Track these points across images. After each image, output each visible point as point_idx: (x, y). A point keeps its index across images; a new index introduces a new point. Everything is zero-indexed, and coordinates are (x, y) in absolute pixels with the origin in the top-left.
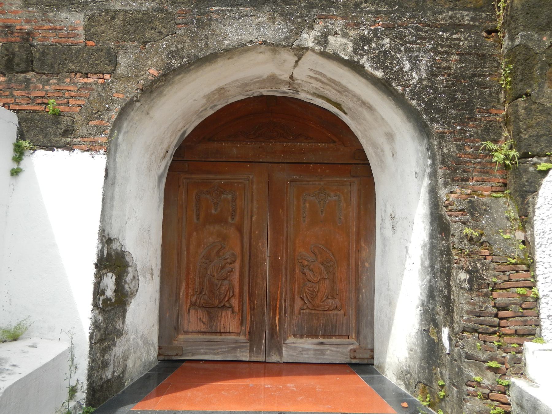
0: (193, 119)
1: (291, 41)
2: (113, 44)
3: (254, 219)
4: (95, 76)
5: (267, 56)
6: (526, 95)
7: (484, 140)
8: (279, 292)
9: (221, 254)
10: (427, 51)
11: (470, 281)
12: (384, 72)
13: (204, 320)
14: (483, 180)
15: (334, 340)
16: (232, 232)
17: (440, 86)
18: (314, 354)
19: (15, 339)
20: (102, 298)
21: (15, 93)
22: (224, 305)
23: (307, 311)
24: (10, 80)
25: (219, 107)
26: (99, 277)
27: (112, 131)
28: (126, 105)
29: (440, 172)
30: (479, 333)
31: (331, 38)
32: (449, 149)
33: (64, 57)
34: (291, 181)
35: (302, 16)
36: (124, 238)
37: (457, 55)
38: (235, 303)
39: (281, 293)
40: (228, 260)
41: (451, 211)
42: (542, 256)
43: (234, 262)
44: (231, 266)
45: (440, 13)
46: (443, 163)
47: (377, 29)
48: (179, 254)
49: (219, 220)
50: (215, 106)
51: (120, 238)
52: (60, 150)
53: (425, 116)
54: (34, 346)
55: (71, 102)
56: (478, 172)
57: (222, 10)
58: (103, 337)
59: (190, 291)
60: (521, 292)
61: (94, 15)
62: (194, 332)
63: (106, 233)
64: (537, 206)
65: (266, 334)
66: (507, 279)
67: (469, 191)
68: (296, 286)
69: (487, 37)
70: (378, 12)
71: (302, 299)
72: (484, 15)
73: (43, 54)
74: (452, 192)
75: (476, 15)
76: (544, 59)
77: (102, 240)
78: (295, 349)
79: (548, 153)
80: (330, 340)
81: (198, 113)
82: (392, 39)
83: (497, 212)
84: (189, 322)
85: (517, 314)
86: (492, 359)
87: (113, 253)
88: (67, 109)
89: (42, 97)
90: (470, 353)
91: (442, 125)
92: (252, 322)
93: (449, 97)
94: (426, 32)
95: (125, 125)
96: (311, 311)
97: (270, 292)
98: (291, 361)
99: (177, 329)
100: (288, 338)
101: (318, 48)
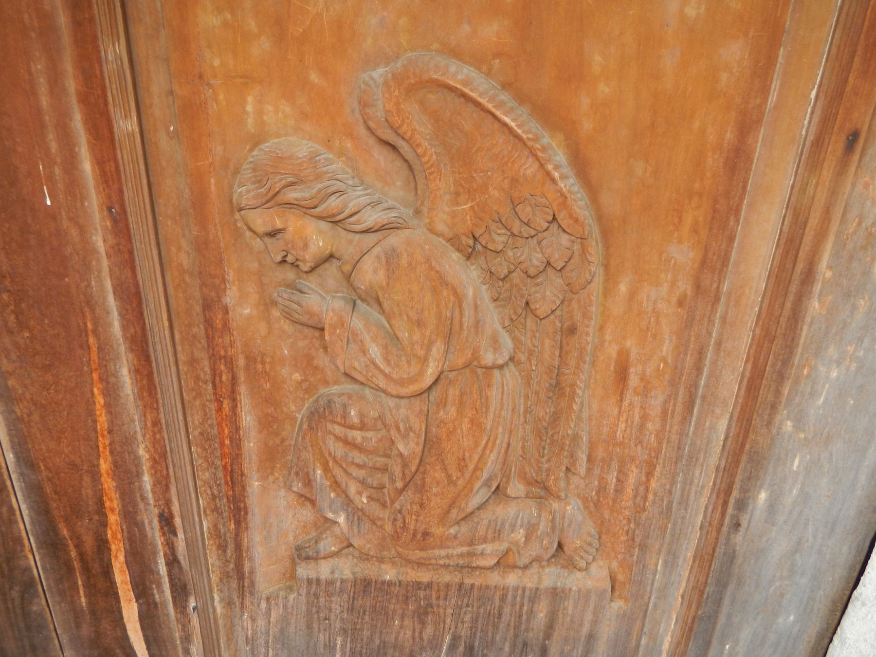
8: (104, 466)
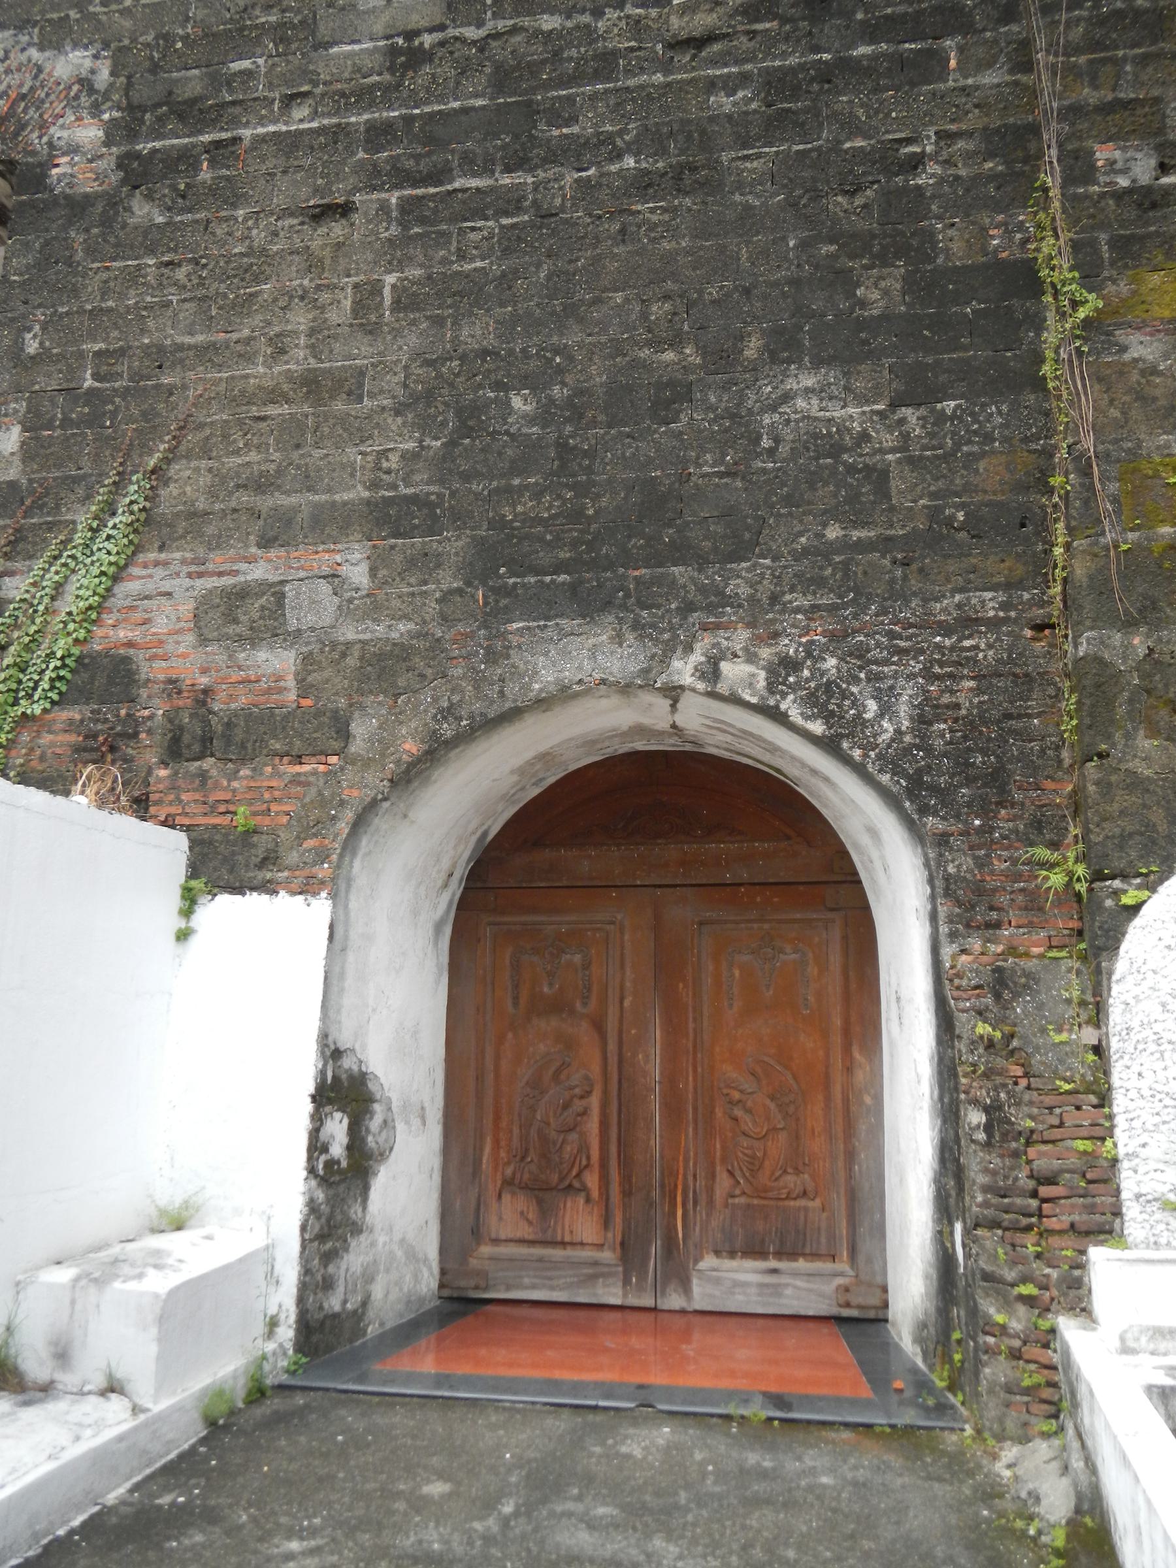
0: (500, 808)
1: (652, 675)
2: (342, 702)
3: (627, 1003)
4: (313, 760)
5: (615, 700)
6: (1101, 756)
9: (563, 1077)
10: (911, 676)
11: (988, 1128)
12: (827, 723)
13: (530, 1216)
14: (1031, 925)
15: (801, 1264)
16: (584, 1032)
17: (938, 743)
18: (759, 1295)
19: (179, 1226)
20: (323, 1158)
21: (184, 797)
22: (570, 1186)
23: (742, 1200)
24: (176, 773)
25: (552, 780)
26: (318, 1120)
27: (341, 856)
28: (364, 809)
29: (942, 911)
30: (1006, 1229)
31: (724, 666)
32: (959, 867)
33: (262, 729)
34: (701, 924)
35: (672, 628)
36: (364, 1047)
37: (973, 678)
38: (592, 1180)
39: (686, 1160)
40: (577, 1091)
41: (958, 988)
42: (1124, 1075)
43: (587, 1094)
44: (584, 1102)
45: (937, 600)
46: (947, 893)
47: (812, 642)
48: (480, 1078)
49: (558, 1006)
50: (541, 780)
51: (357, 1047)
52: (255, 894)
53: (907, 804)
54: (209, 1238)
55: (275, 808)
56: (1020, 909)
57: (528, 628)
58: (326, 1230)
59: (503, 1154)
60: (1081, 1148)
61: (311, 653)
62: (511, 1241)
63: (330, 1039)
64: (1114, 978)
65: (655, 1248)
66: (1056, 1122)
67: (1000, 948)
68: (718, 1146)
69: (1033, 639)
70: (815, 608)
71: (731, 1173)
72: (1026, 596)
73: (229, 725)
74: (964, 951)
75: (1010, 596)
76: (1136, 682)
77: (323, 1053)
78: (718, 1281)
79: (1144, 871)
80: (794, 1265)
81: (507, 798)
82: (842, 659)
83: (1049, 989)
84: (500, 1219)
85: (1075, 1192)
86: (1024, 1279)
87: (344, 1076)
88: (267, 821)
89: (226, 801)
90: (988, 1268)
91: (944, 818)
92: (627, 1221)
93: (957, 764)
94: (909, 638)
95: (364, 842)
96: (749, 1201)
97: (662, 1157)
98: (709, 1308)
99: (477, 1233)
100: (702, 1258)
101: (701, 686)
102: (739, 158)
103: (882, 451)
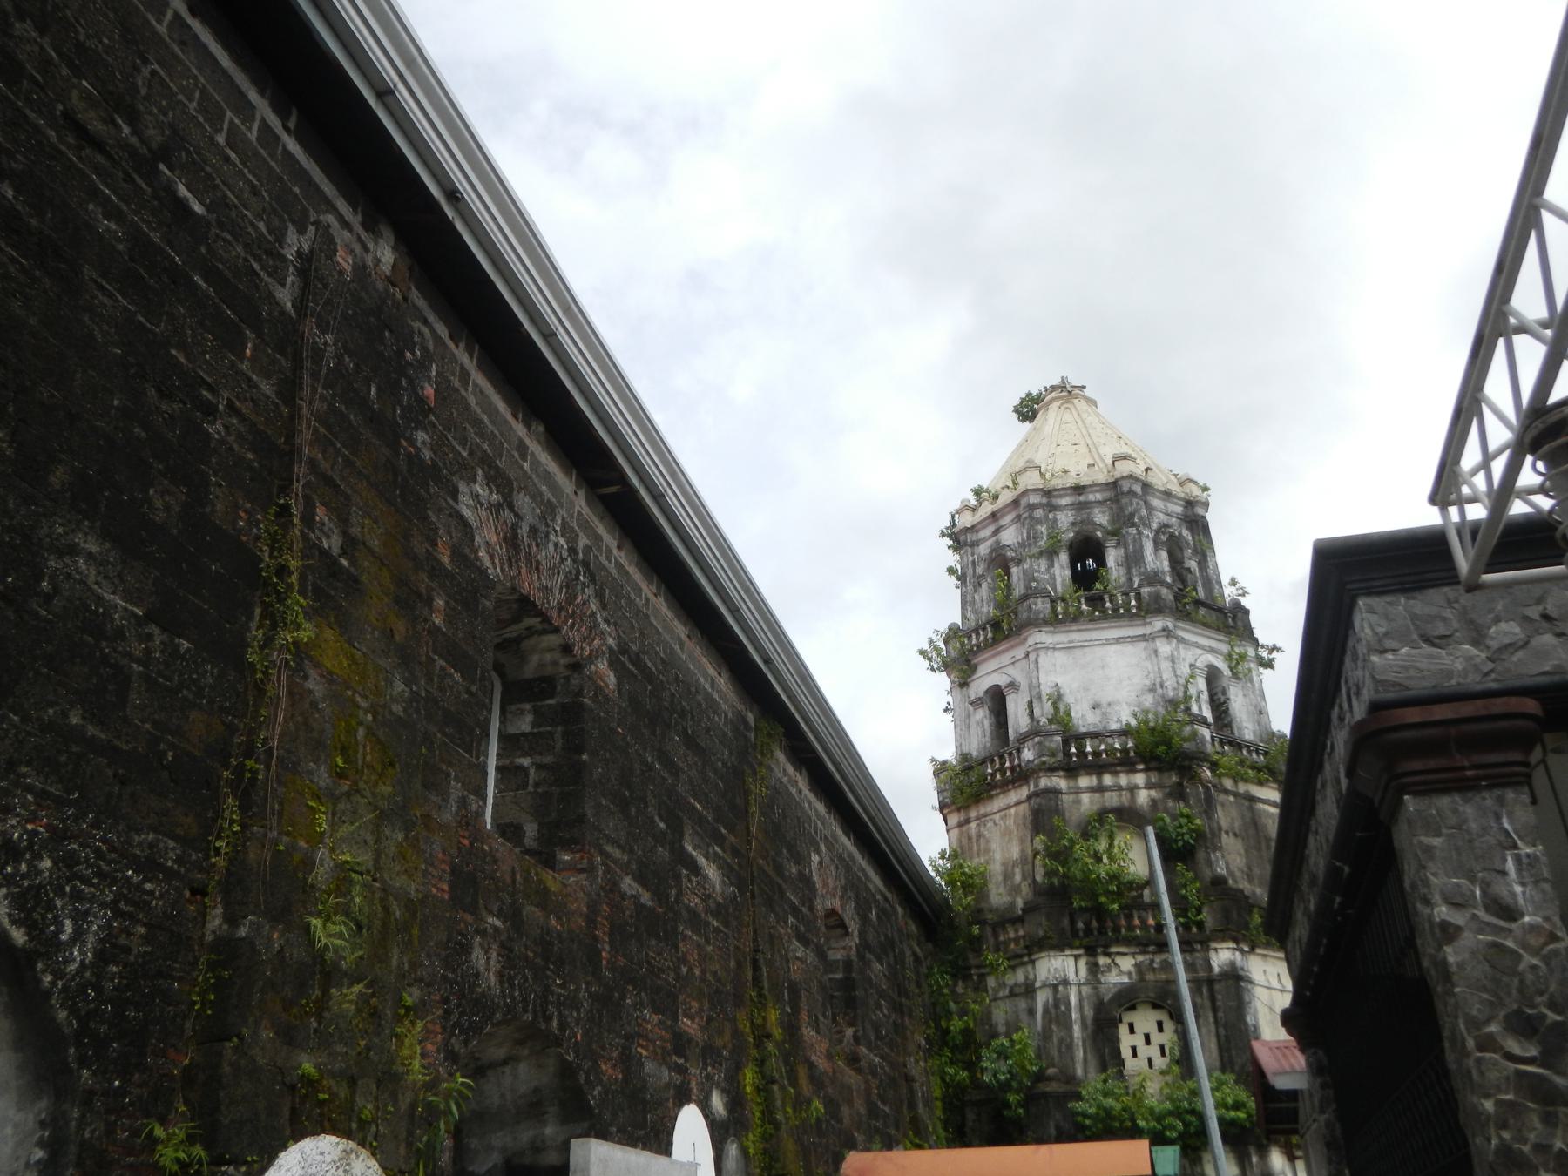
7: (148, 1116)
10: (104, 905)
12: (28, 934)
94: (109, 863)
102: (96, 282)
103: (129, 655)
